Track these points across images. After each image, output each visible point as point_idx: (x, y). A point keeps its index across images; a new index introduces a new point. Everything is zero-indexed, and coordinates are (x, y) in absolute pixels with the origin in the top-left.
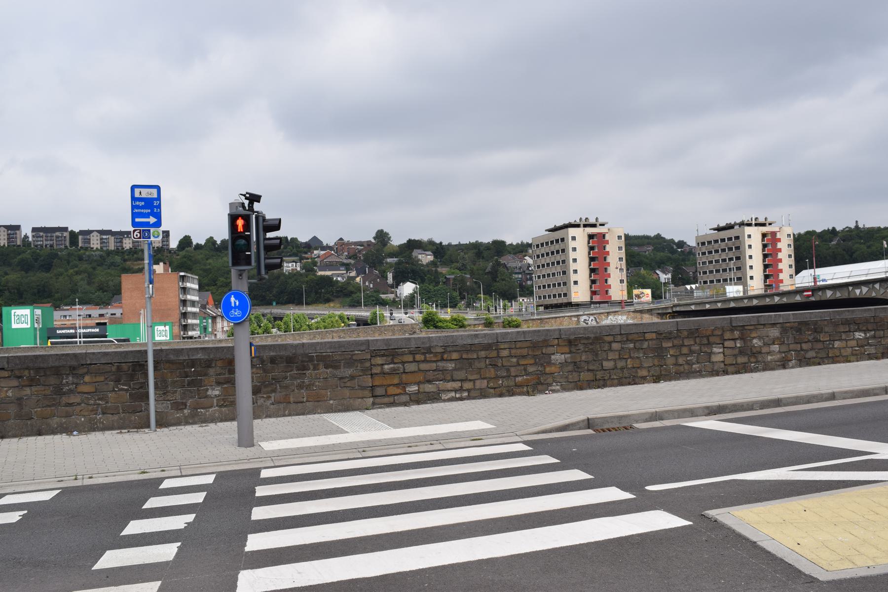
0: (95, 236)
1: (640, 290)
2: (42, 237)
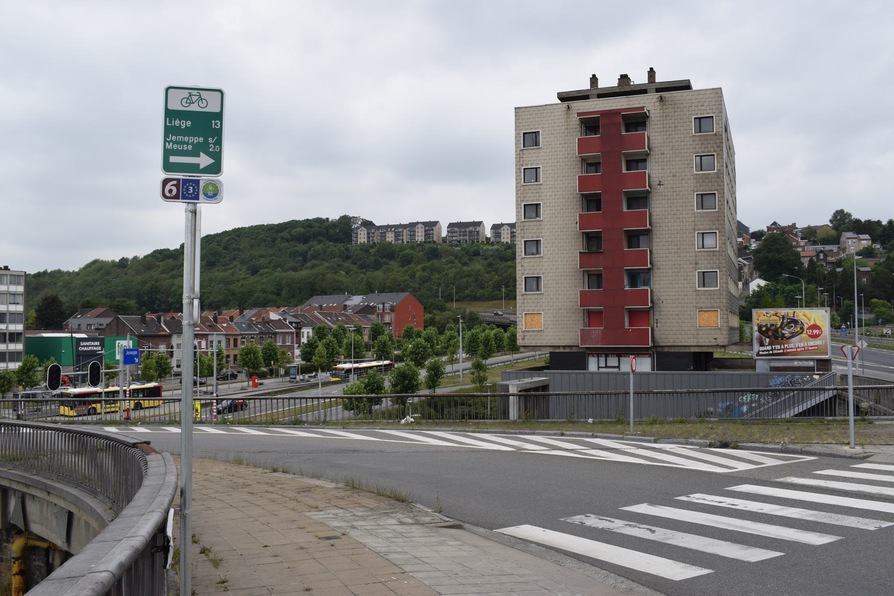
0: (506, 229)
1: (783, 311)
2: (455, 232)
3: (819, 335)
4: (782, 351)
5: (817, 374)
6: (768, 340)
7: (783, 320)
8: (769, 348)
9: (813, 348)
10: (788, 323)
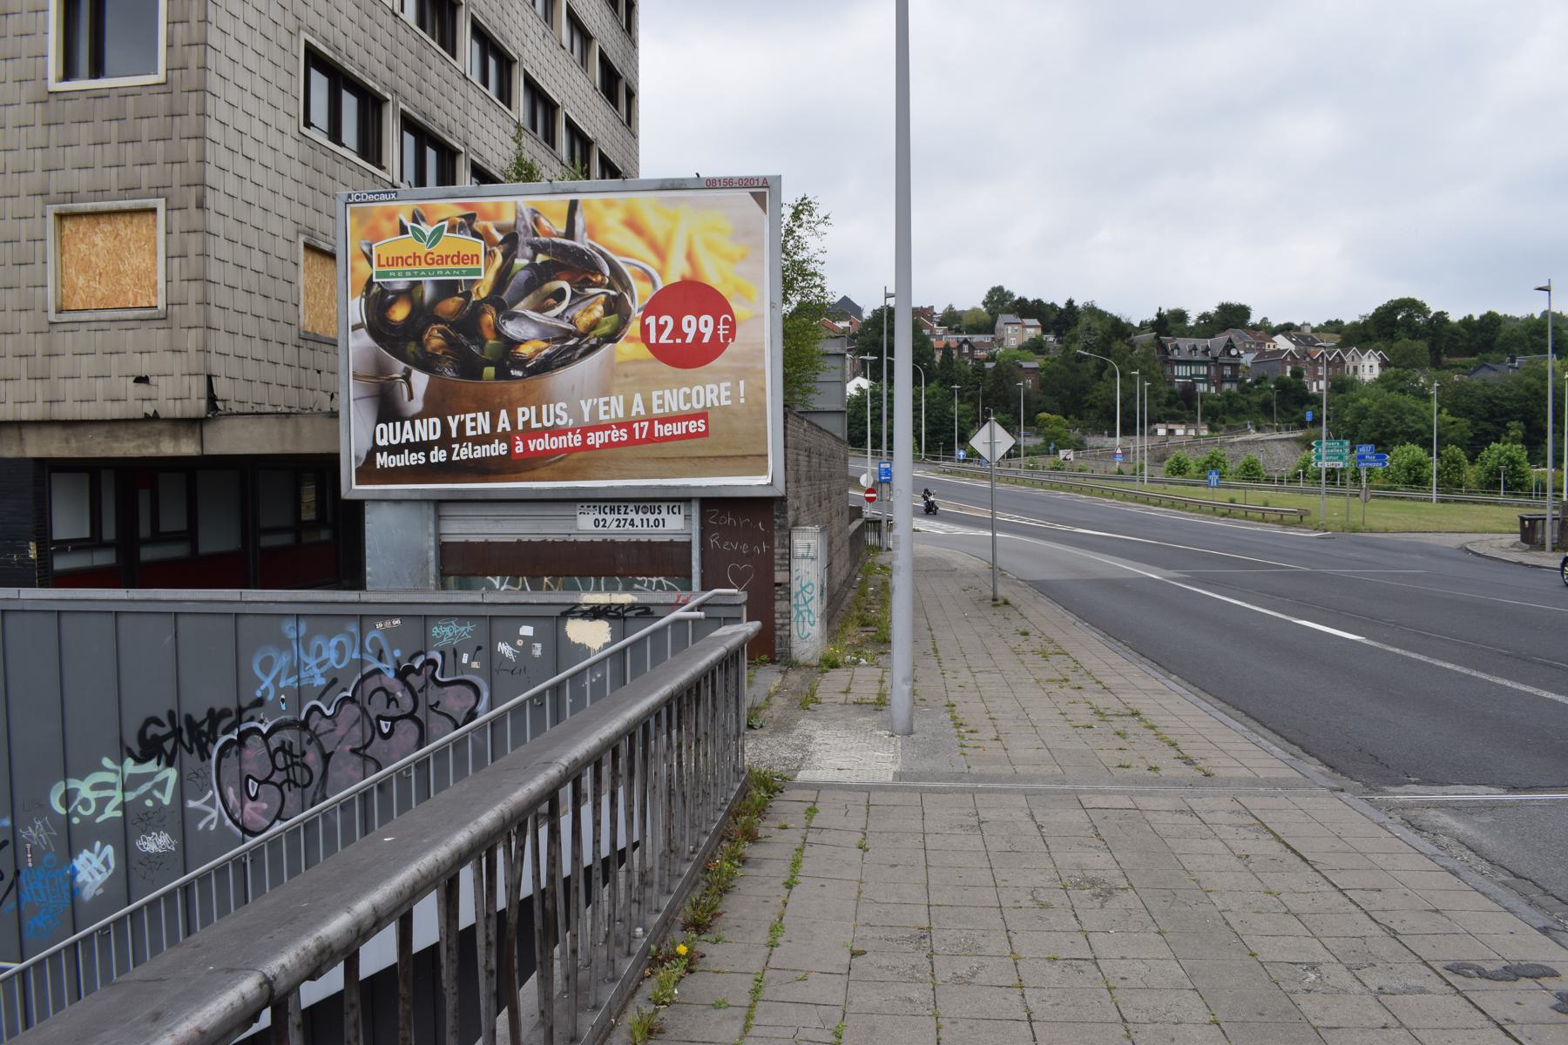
3: (713, 349)
4: (499, 449)
5: (596, 613)
6: (420, 380)
7: (509, 255)
8: (428, 430)
9: (679, 429)
10: (539, 275)
